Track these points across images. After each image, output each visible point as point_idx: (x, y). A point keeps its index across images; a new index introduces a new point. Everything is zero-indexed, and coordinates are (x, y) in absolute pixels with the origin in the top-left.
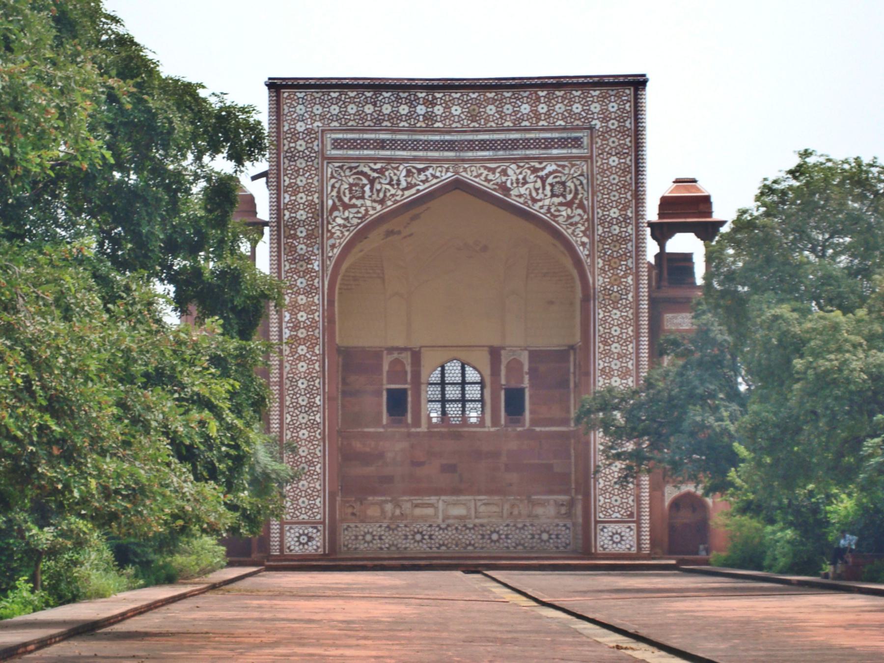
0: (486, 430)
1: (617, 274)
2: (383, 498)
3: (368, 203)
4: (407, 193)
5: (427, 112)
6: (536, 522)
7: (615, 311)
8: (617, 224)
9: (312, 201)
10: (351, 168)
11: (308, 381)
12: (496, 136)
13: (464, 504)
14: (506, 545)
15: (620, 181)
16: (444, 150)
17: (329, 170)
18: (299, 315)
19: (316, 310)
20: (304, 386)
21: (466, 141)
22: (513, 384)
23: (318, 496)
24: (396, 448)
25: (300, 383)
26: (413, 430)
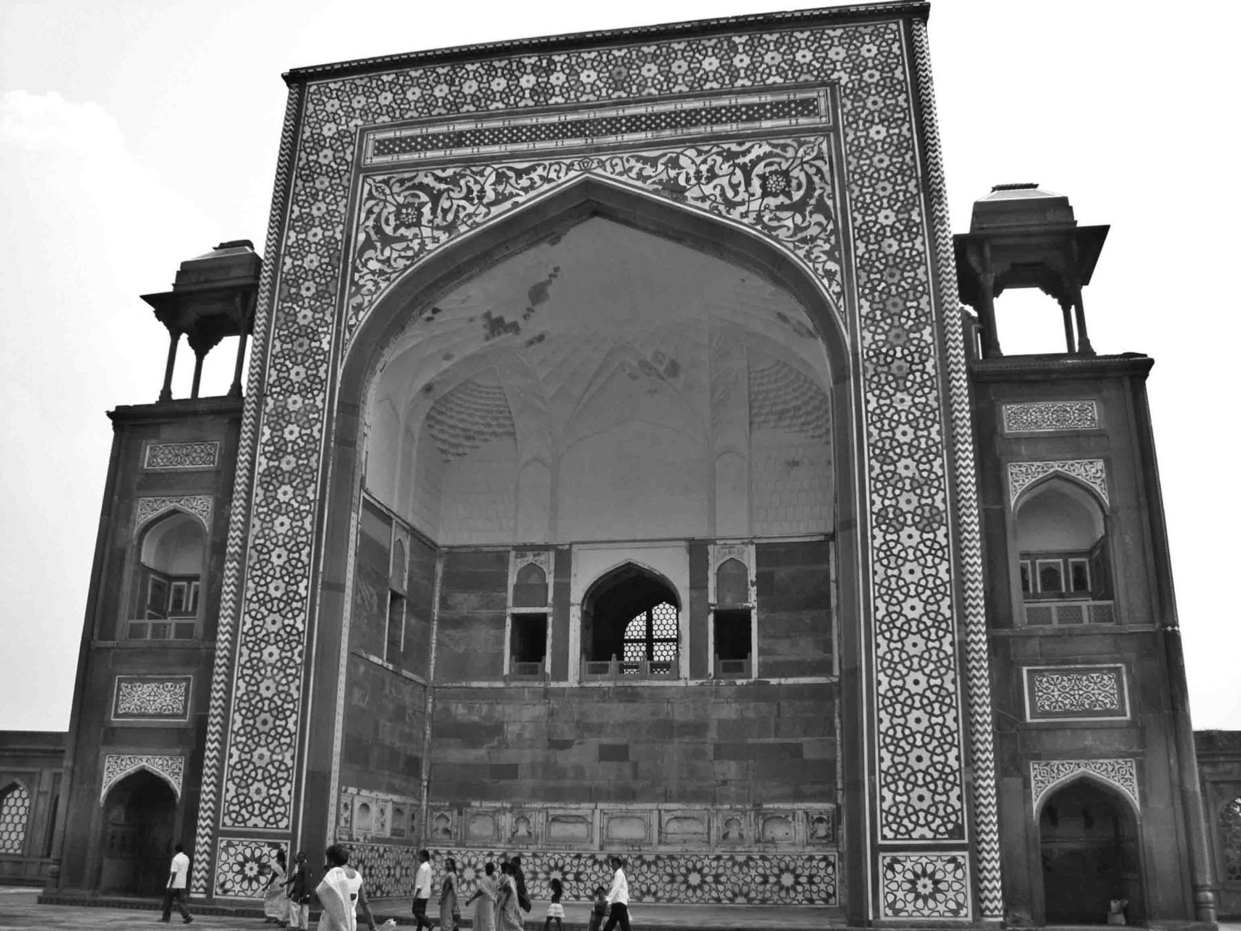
0: (682, 683)
1: (902, 325)
2: (498, 805)
3: (426, 232)
4: (495, 210)
5: (538, 84)
6: (770, 852)
7: (899, 395)
8: (893, 236)
9: (332, 237)
10: (402, 182)
11: (290, 551)
12: (658, 108)
13: (640, 818)
14: (714, 894)
15: (893, 164)
16: (565, 136)
17: (367, 188)
18: (286, 431)
19: (317, 420)
20: (281, 562)
21: (605, 119)
22: (729, 603)
23: (287, 780)
24: (523, 716)
25: (274, 554)
26: (554, 685)
